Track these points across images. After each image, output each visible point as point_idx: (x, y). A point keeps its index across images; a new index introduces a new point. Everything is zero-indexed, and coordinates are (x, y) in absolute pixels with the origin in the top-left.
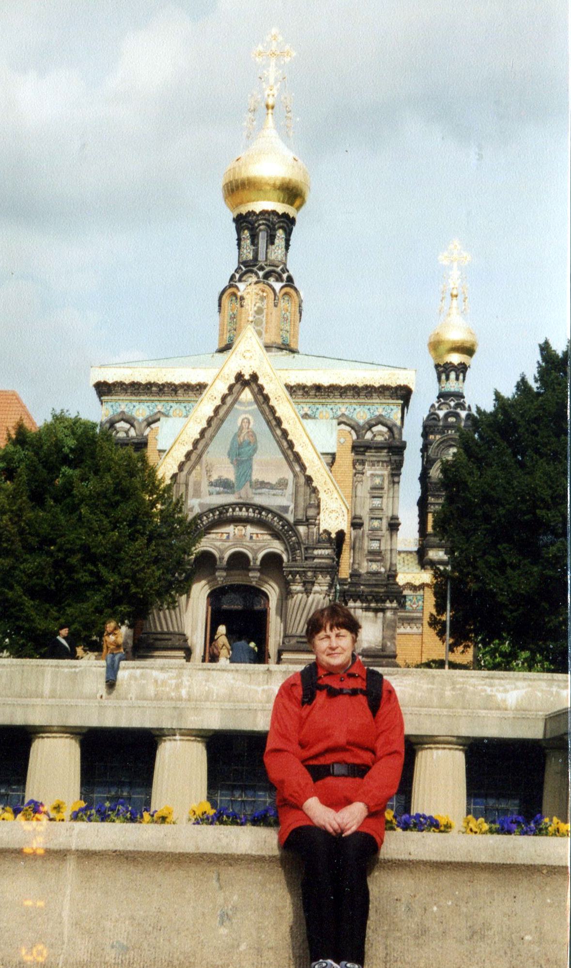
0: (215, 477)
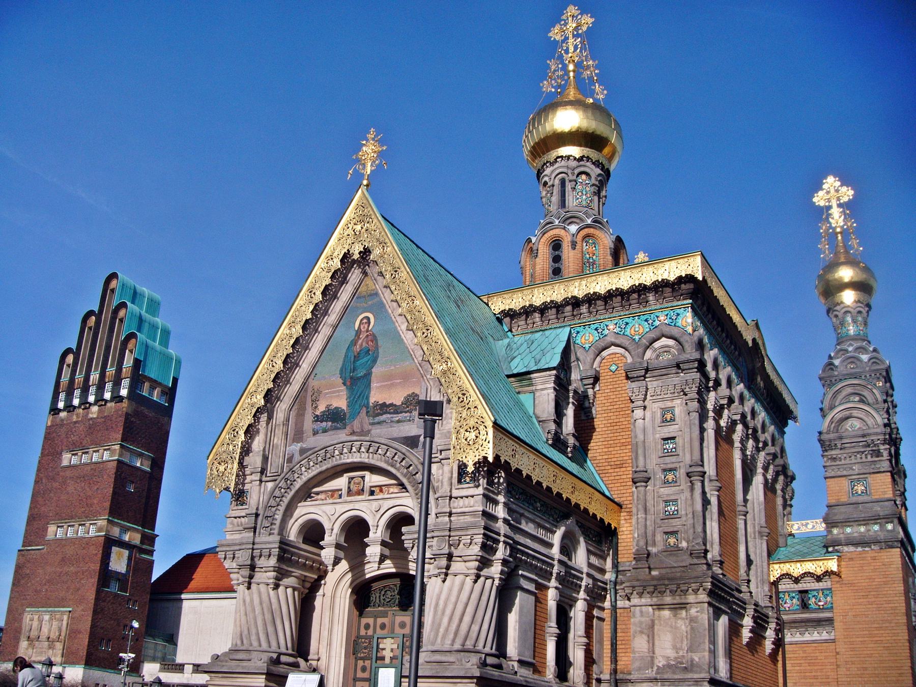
0: (322, 408)
